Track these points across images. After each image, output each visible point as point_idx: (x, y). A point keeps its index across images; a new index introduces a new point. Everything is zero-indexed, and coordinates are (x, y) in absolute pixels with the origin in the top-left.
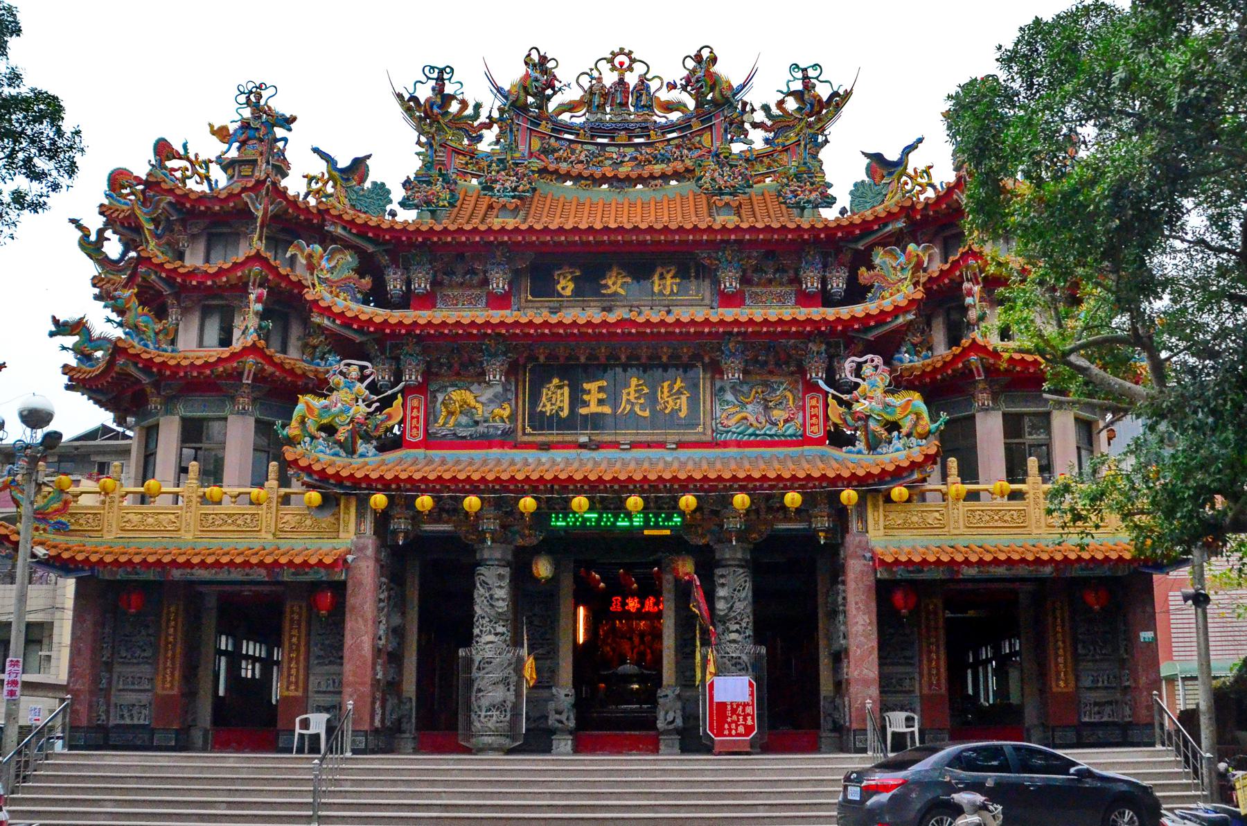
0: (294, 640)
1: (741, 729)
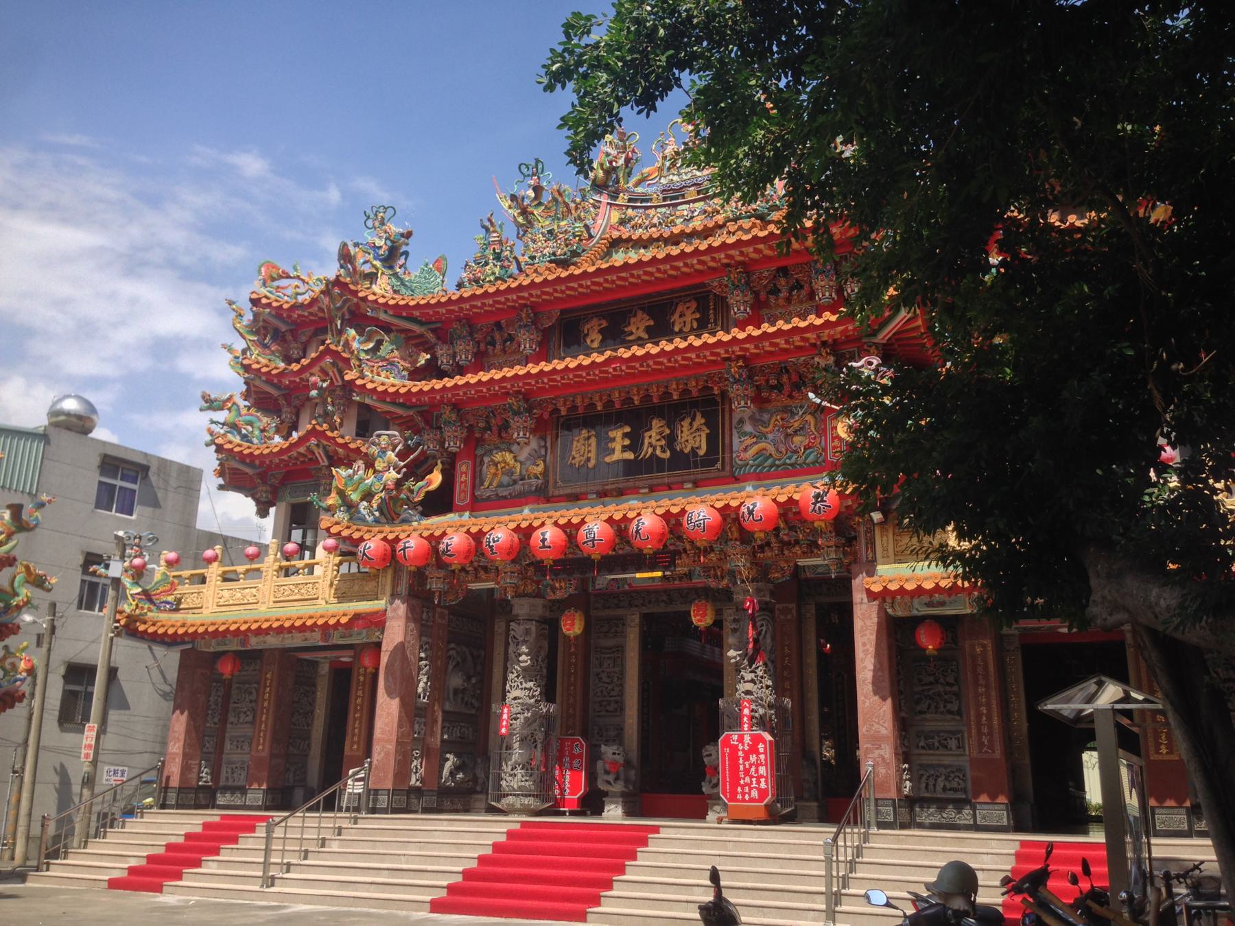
0: (359, 701)
1: (755, 794)
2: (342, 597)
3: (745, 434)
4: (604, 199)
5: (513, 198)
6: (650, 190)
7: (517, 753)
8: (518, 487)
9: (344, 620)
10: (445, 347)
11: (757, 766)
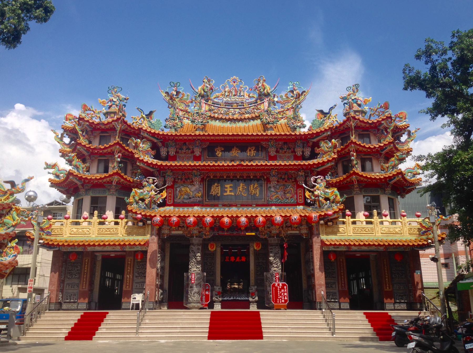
0: (129, 270)
1: (283, 301)
2: (129, 234)
3: (272, 191)
4: (203, 101)
5: (167, 93)
6: (220, 101)
7: (195, 289)
8: (191, 200)
9: (142, 243)
10: (165, 149)
11: (284, 293)
